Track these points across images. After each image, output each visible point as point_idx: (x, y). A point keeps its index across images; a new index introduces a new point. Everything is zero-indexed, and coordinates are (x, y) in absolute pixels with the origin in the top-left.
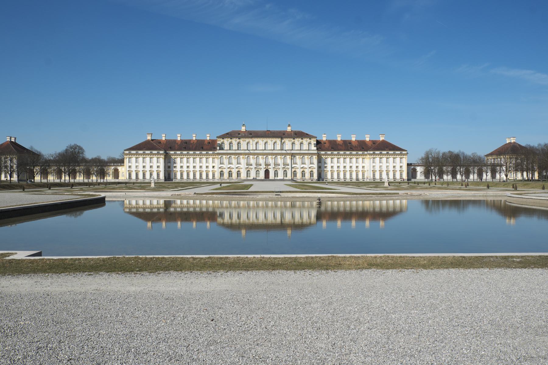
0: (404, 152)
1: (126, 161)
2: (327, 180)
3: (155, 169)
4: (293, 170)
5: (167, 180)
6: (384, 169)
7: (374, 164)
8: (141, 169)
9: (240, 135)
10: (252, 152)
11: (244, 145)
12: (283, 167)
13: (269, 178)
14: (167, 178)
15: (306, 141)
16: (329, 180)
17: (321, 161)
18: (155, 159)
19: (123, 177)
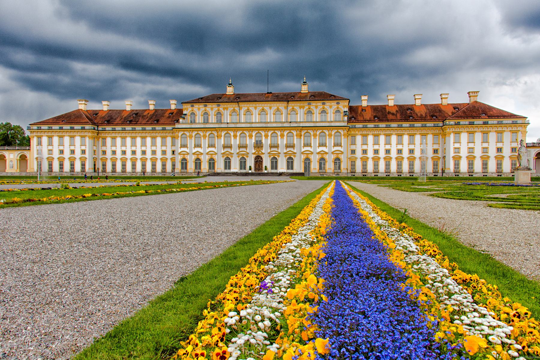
0: (520, 121)
1: (34, 142)
2: (366, 175)
3: (78, 154)
4: (303, 157)
5: (101, 173)
6: (478, 153)
7: (457, 145)
8: (56, 155)
9: (220, 100)
10: (233, 126)
11: (227, 118)
12: (285, 151)
13: (262, 170)
14: (100, 171)
15: (331, 107)
16: (357, 174)
17: (355, 141)
18: (78, 139)
19: (32, 167)
